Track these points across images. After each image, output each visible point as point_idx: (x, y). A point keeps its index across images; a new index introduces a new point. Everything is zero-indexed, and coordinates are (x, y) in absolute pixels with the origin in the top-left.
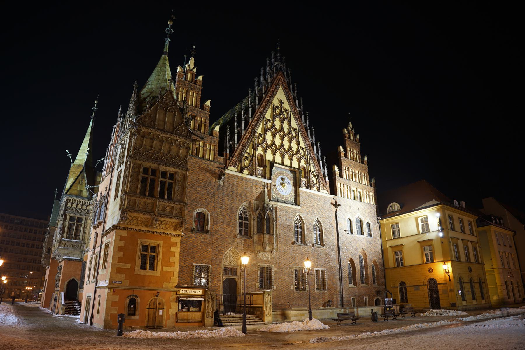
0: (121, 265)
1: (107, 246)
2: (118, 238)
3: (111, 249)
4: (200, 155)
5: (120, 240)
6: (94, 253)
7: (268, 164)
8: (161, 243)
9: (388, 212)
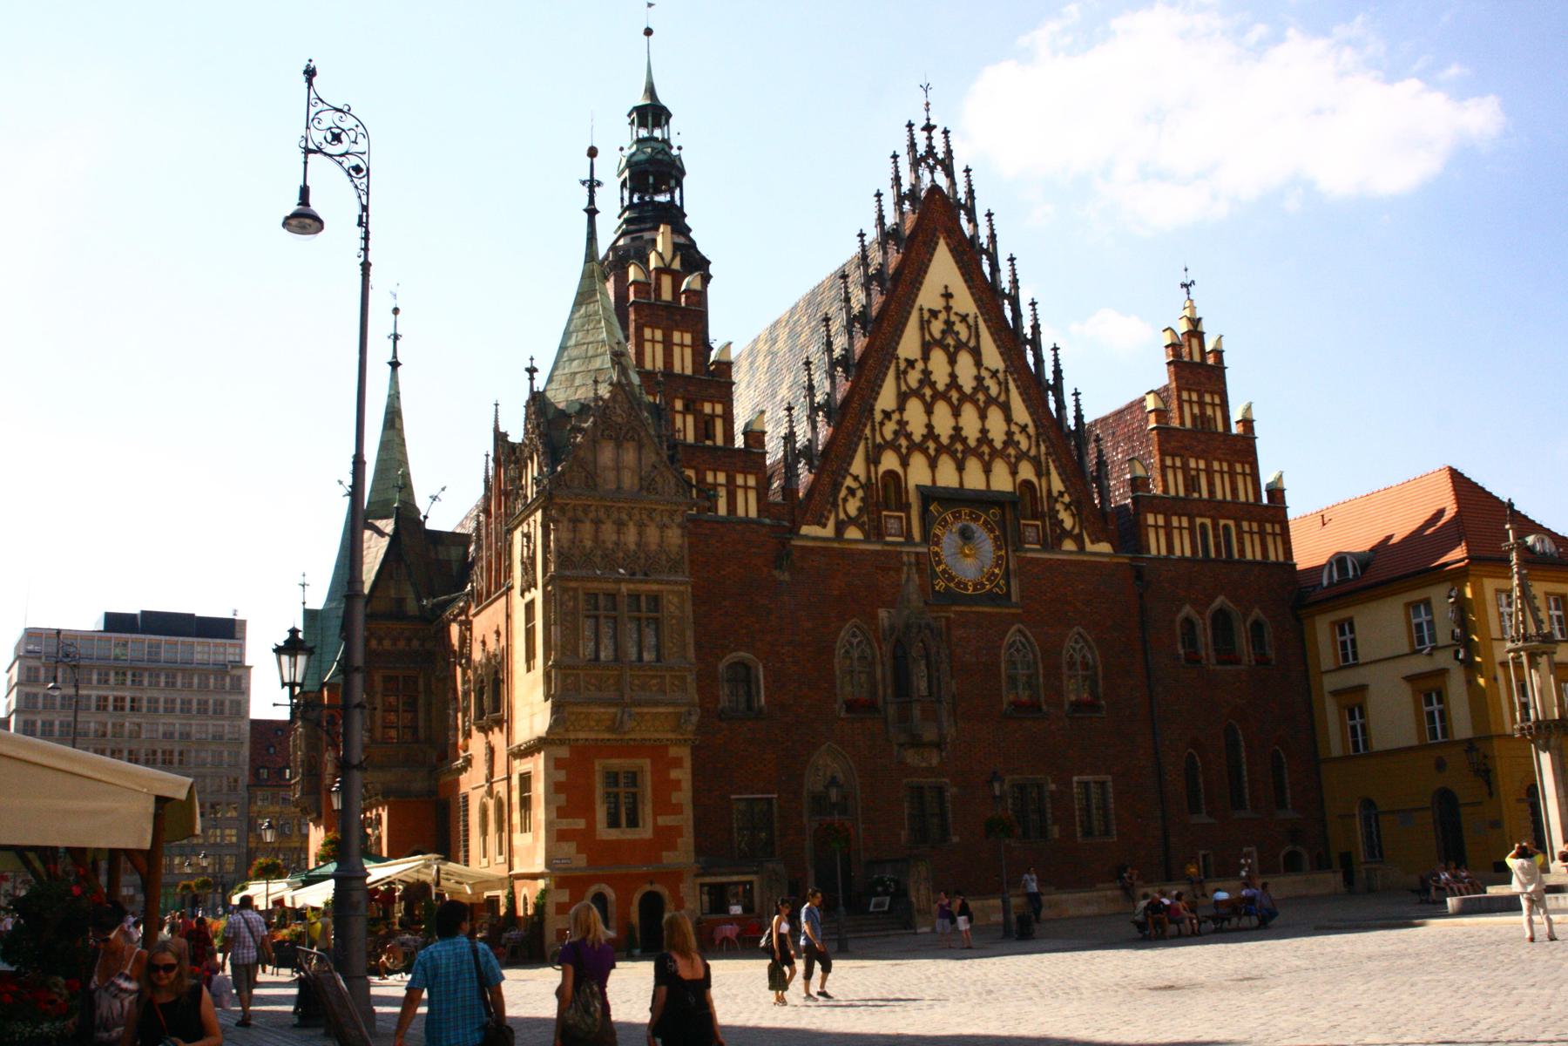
0: (565, 824)
1: (526, 780)
2: (552, 764)
3: (539, 789)
4: (722, 509)
6: (490, 793)
7: (913, 498)
8: (646, 763)
9: (1325, 582)
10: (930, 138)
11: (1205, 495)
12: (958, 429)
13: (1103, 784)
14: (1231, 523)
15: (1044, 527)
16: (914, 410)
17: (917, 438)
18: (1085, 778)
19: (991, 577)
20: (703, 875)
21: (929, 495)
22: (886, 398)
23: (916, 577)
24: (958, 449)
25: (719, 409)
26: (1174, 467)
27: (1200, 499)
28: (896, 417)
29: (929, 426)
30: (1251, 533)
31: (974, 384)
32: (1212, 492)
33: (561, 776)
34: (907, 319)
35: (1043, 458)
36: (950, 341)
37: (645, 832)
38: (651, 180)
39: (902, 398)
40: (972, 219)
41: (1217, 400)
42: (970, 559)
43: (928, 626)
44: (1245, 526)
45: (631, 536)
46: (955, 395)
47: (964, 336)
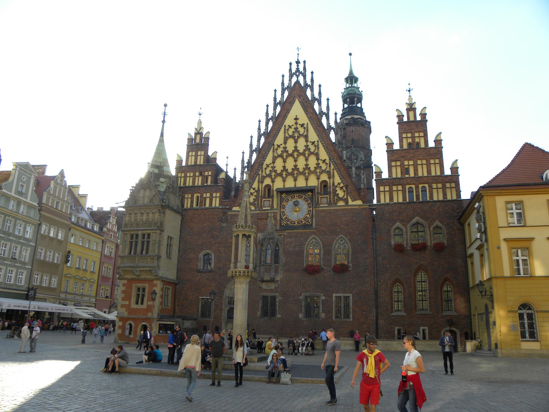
0: (123, 302)
4: (207, 205)
5: (123, 286)
10: (298, 66)
11: (412, 174)
12: (295, 166)
13: (347, 298)
14: (427, 186)
15: (330, 198)
16: (279, 161)
17: (279, 172)
18: (339, 295)
19: (306, 218)
20: (160, 321)
21: (281, 192)
22: (269, 160)
23: (273, 221)
24: (295, 173)
25: (210, 173)
26: (396, 166)
27: (409, 178)
28: (270, 166)
29: (284, 167)
30: (437, 188)
31: (304, 148)
32: (415, 174)
33: (124, 288)
34: (280, 131)
35: (332, 172)
36: (296, 135)
37: (144, 306)
38: (356, 99)
39: (274, 159)
40: (312, 90)
41: (422, 134)
42: (297, 212)
43: (272, 238)
44: (434, 186)
45: (145, 217)
46: (296, 154)
47: (301, 133)
